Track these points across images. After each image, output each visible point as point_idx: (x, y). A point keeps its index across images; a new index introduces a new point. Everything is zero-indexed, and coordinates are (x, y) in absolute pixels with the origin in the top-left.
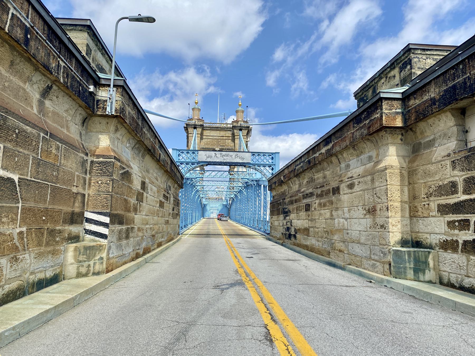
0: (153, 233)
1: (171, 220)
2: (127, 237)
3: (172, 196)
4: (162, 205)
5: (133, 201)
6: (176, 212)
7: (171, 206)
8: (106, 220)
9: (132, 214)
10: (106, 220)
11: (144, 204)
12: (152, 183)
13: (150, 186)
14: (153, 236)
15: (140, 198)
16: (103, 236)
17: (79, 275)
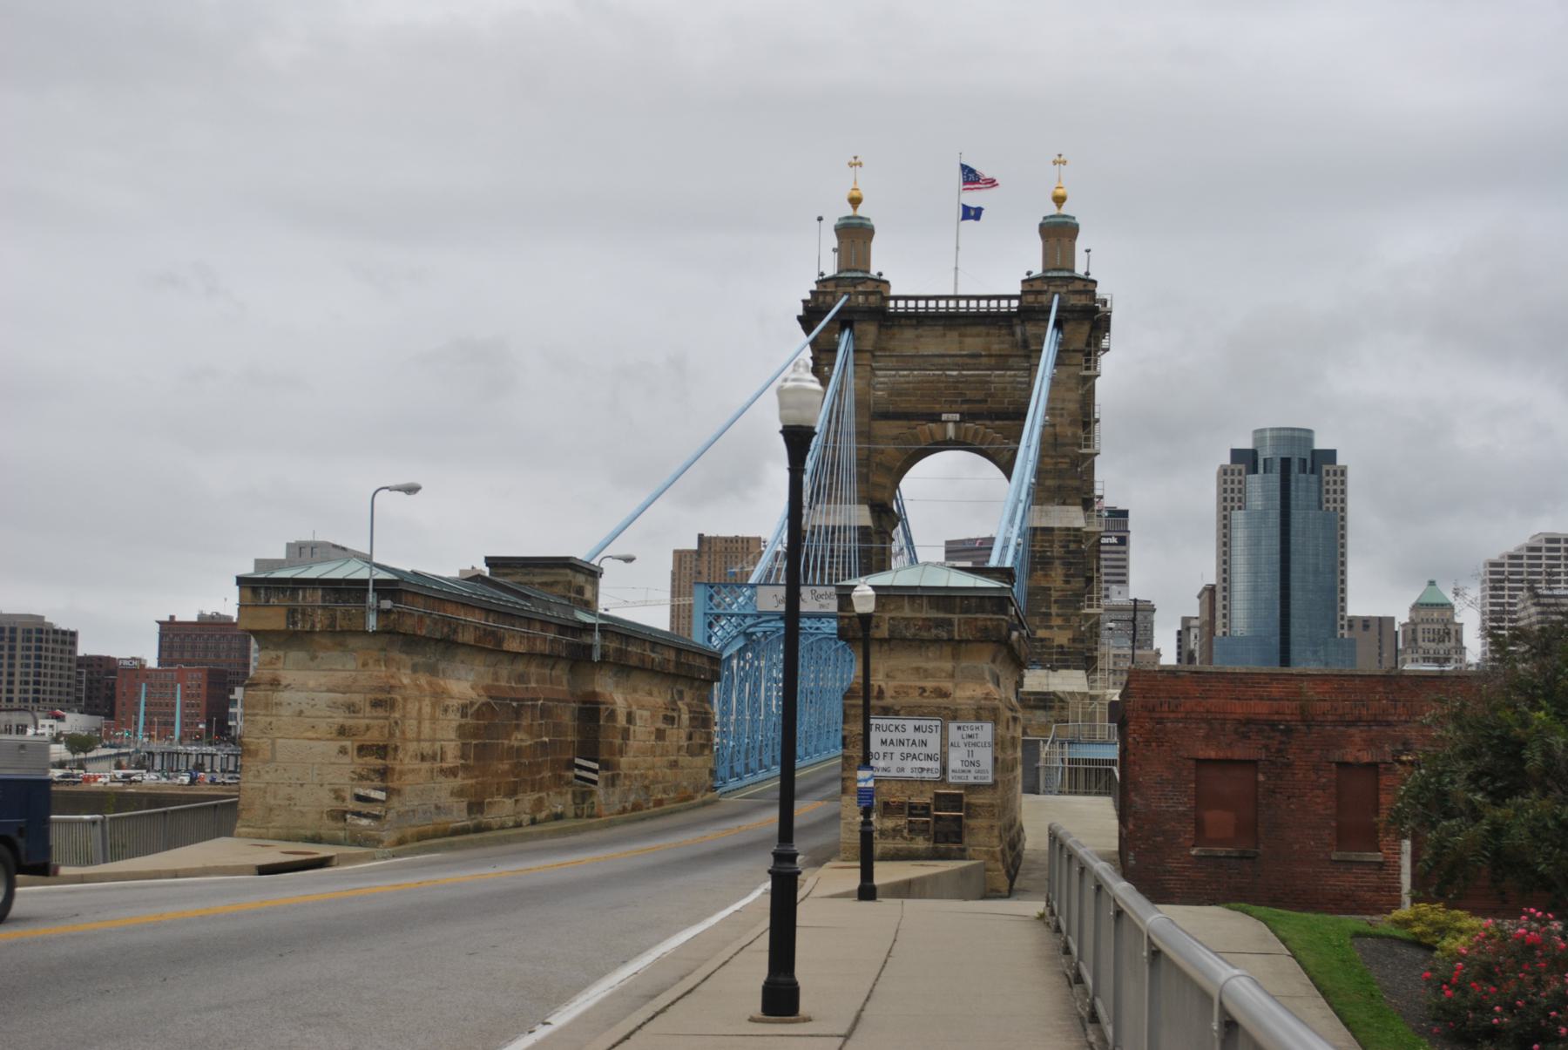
0: (647, 782)
1: (685, 760)
2: (613, 785)
3: (684, 709)
4: (660, 735)
5: (618, 741)
6: (697, 740)
7: (683, 733)
8: (596, 766)
9: (617, 758)
10: (596, 766)
11: (631, 742)
12: (642, 707)
13: (638, 713)
14: (647, 787)
15: (626, 734)
16: (595, 782)
17: (577, 816)
